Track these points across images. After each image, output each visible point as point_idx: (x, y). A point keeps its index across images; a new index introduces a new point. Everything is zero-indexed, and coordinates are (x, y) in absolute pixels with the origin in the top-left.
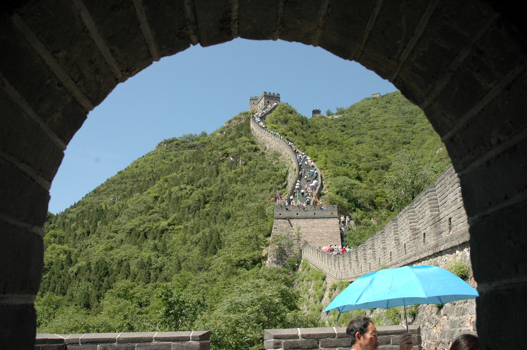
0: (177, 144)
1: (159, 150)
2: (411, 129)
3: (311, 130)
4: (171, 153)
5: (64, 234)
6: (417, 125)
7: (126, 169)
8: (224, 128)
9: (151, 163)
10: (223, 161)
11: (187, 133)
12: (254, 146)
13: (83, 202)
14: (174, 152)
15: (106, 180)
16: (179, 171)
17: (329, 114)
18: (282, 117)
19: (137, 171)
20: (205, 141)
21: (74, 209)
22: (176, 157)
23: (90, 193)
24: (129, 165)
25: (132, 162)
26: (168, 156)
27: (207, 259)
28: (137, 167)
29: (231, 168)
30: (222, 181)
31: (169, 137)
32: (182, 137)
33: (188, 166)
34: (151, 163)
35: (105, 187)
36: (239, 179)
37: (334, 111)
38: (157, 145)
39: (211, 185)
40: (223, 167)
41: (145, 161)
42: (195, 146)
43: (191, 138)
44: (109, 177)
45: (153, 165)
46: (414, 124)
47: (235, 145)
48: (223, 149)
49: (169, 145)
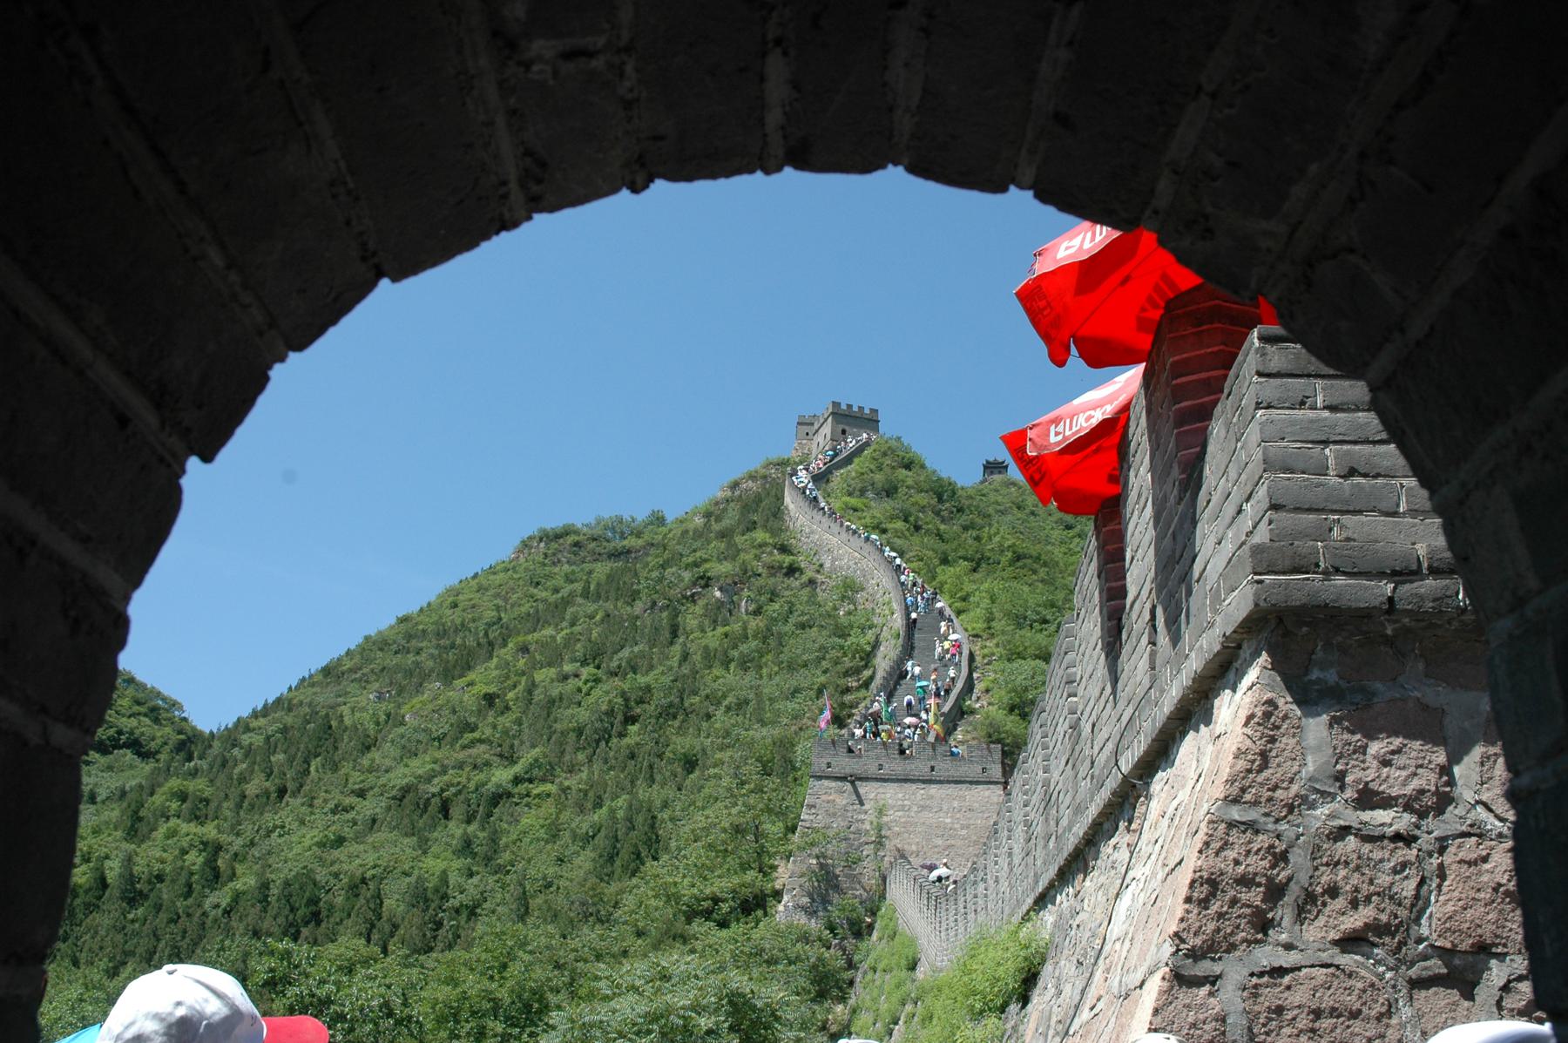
0: (577, 544)
1: (522, 560)
3: (964, 519)
4: (556, 570)
5: (208, 792)
8: (717, 503)
9: (497, 595)
10: (693, 599)
11: (608, 513)
12: (788, 559)
13: (290, 701)
14: (566, 567)
15: (361, 640)
16: (564, 624)
21: (262, 721)
23: (311, 676)
24: (433, 598)
26: (549, 576)
27: (611, 889)
28: (455, 605)
29: (715, 621)
30: (685, 657)
31: (554, 523)
32: (593, 522)
33: (591, 607)
34: (497, 595)
35: (357, 659)
36: (735, 653)
38: (517, 543)
39: (651, 667)
40: (691, 618)
42: (629, 552)
43: (618, 527)
44: (373, 632)
45: (501, 603)
47: (731, 554)
48: (696, 565)
49: (554, 545)
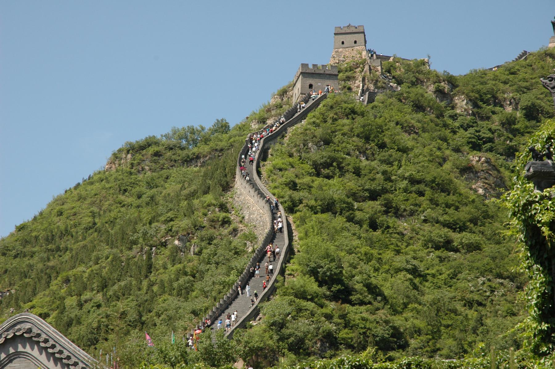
0: (157, 154)
1: (114, 170)
3: (384, 154)
4: (140, 177)
7: (35, 218)
8: (269, 110)
9: (93, 203)
10: (164, 245)
11: (183, 123)
12: (223, 215)
14: (149, 173)
16: (91, 263)
18: (319, 132)
19: (60, 223)
22: (151, 188)
25: (50, 200)
26: (134, 184)
28: (60, 213)
31: (138, 136)
32: (171, 133)
34: (93, 203)
36: (175, 285)
38: (109, 155)
40: (161, 258)
41: (81, 198)
42: (198, 157)
43: (192, 136)
45: (96, 209)
49: (138, 156)
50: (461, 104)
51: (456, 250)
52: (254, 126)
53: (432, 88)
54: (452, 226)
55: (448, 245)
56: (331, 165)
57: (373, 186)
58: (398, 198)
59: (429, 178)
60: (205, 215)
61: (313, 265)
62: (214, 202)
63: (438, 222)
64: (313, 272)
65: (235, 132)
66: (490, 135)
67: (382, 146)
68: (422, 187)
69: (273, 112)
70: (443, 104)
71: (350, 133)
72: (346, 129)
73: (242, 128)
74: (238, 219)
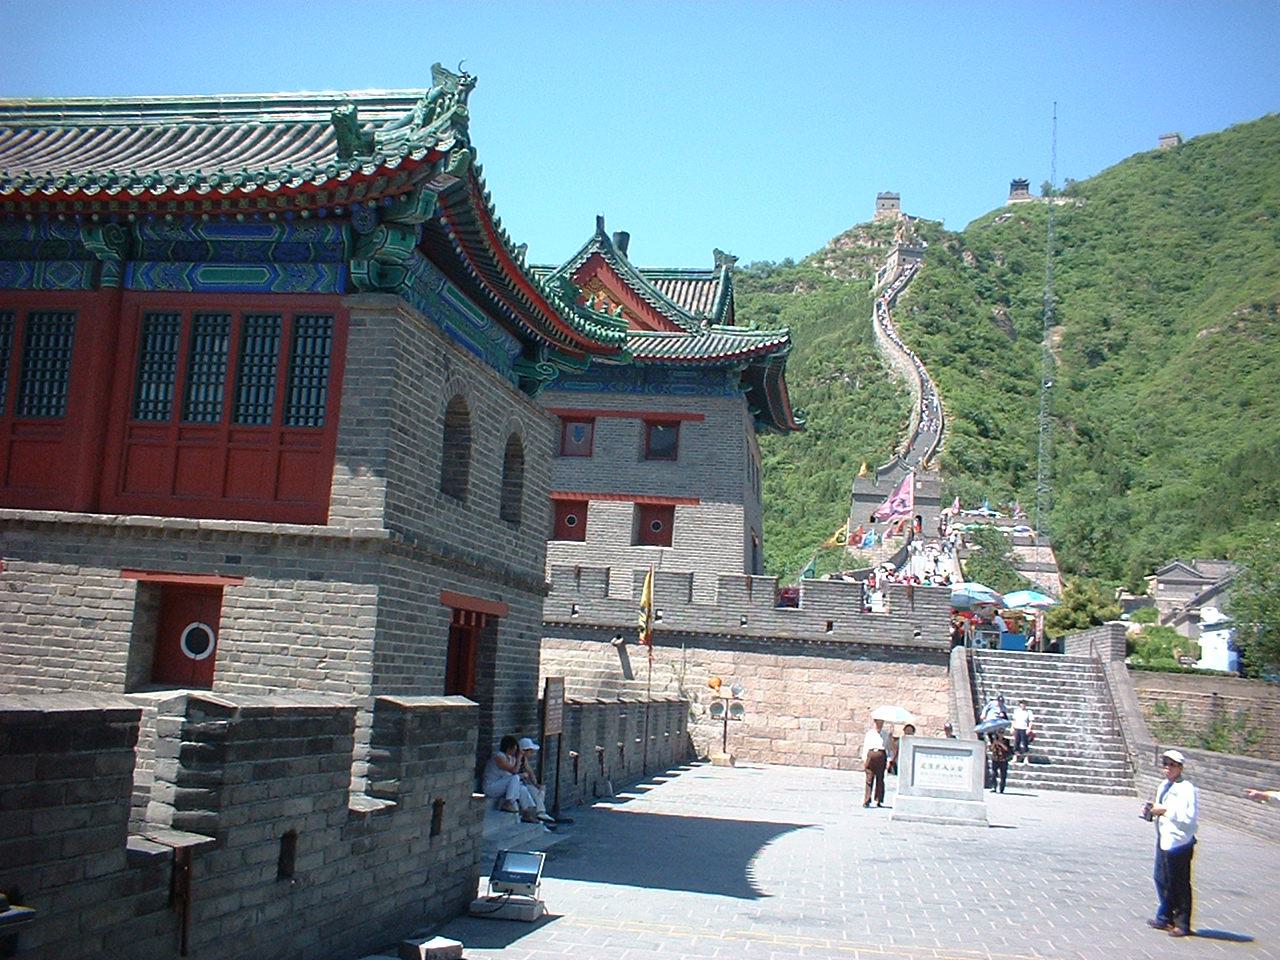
0: (741, 281)
2: (1204, 254)
3: (963, 318)
6: (1220, 244)
17: (1047, 192)
20: (791, 278)
27: (826, 507)
37: (1060, 185)
43: (769, 270)
46: (1216, 241)
47: (851, 357)
50: (968, 259)
51: (1019, 393)
52: (815, 265)
53: (947, 245)
54: (1015, 375)
55: (1012, 389)
56: (932, 325)
57: (961, 342)
58: (978, 352)
59: (996, 339)
60: (863, 361)
61: (966, 411)
62: (869, 352)
63: (1006, 372)
64: (966, 417)
65: (801, 268)
66: (989, 285)
67: (961, 312)
68: (991, 344)
69: (829, 256)
70: (955, 257)
71: (940, 301)
72: (936, 297)
73: (805, 264)
74: (887, 366)
